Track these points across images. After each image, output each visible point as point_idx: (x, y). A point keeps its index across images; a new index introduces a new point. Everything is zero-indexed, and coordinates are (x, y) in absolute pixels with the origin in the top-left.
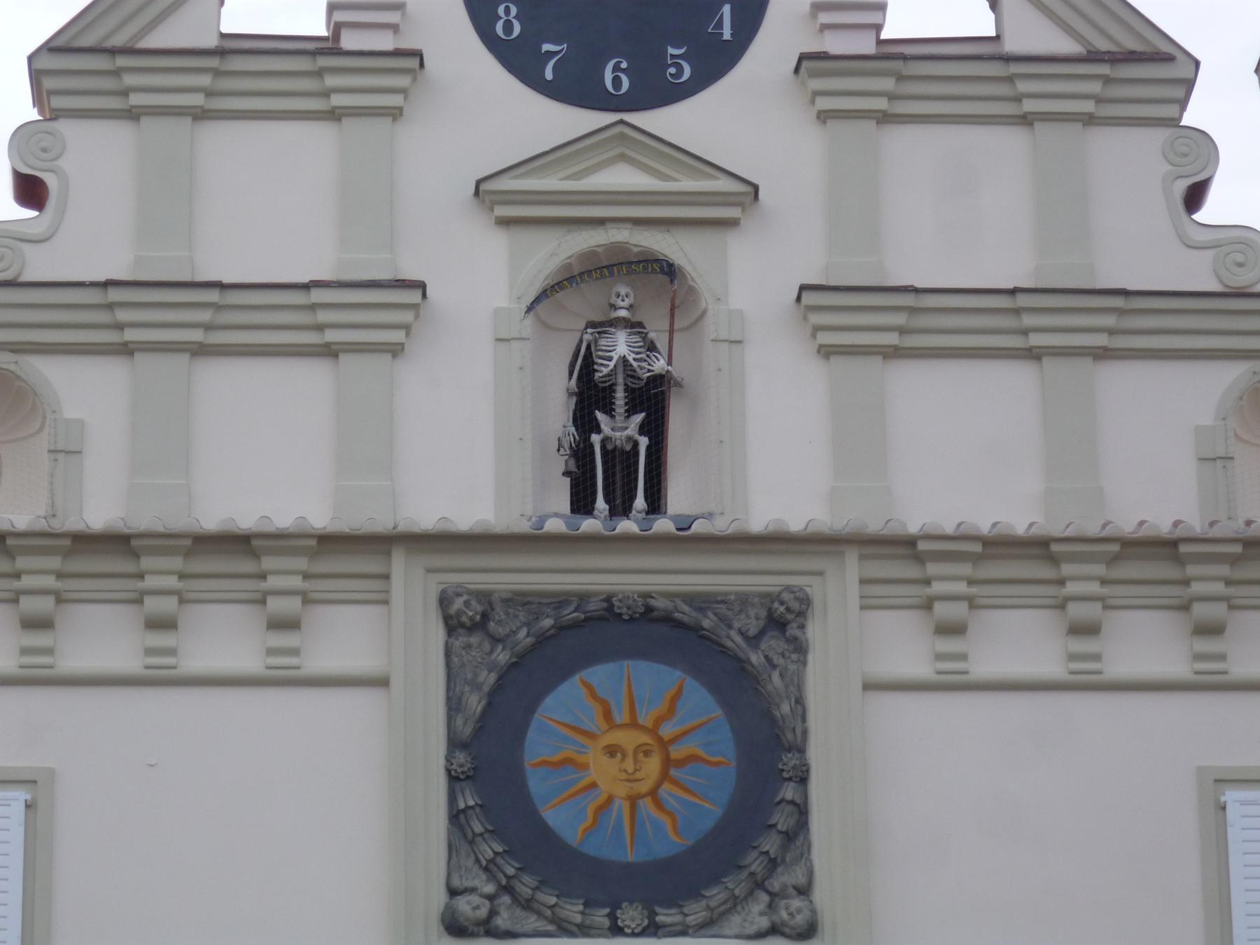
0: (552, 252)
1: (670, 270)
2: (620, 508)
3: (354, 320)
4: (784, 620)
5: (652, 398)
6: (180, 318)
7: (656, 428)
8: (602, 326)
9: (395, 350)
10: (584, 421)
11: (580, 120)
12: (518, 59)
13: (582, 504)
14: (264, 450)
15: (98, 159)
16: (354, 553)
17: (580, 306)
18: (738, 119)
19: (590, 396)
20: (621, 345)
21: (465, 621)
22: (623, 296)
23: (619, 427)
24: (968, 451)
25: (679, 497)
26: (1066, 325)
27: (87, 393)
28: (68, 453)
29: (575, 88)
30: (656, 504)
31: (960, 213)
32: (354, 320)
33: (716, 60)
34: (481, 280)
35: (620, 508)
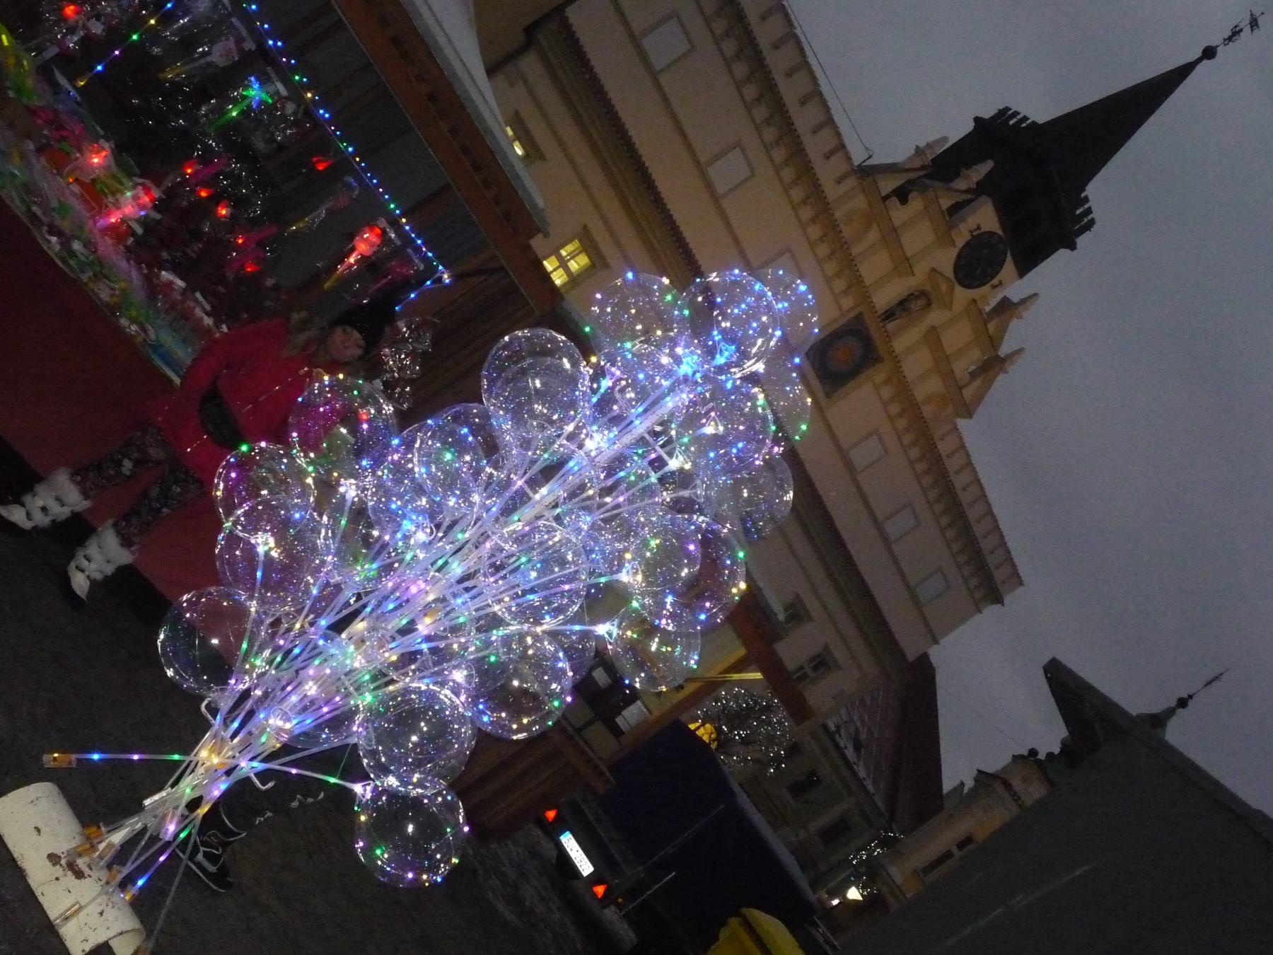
0: (928, 288)
3: (903, 265)
4: (878, 360)
11: (949, 272)
12: (959, 257)
14: (874, 266)
16: (866, 298)
18: (962, 295)
19: (902, 303)
21: (859, 318)
24: (916, 364)
26: (943, 364)
27: (873, 235)
31: (958, 336)
32: (903, 265)
34: (917, 280)
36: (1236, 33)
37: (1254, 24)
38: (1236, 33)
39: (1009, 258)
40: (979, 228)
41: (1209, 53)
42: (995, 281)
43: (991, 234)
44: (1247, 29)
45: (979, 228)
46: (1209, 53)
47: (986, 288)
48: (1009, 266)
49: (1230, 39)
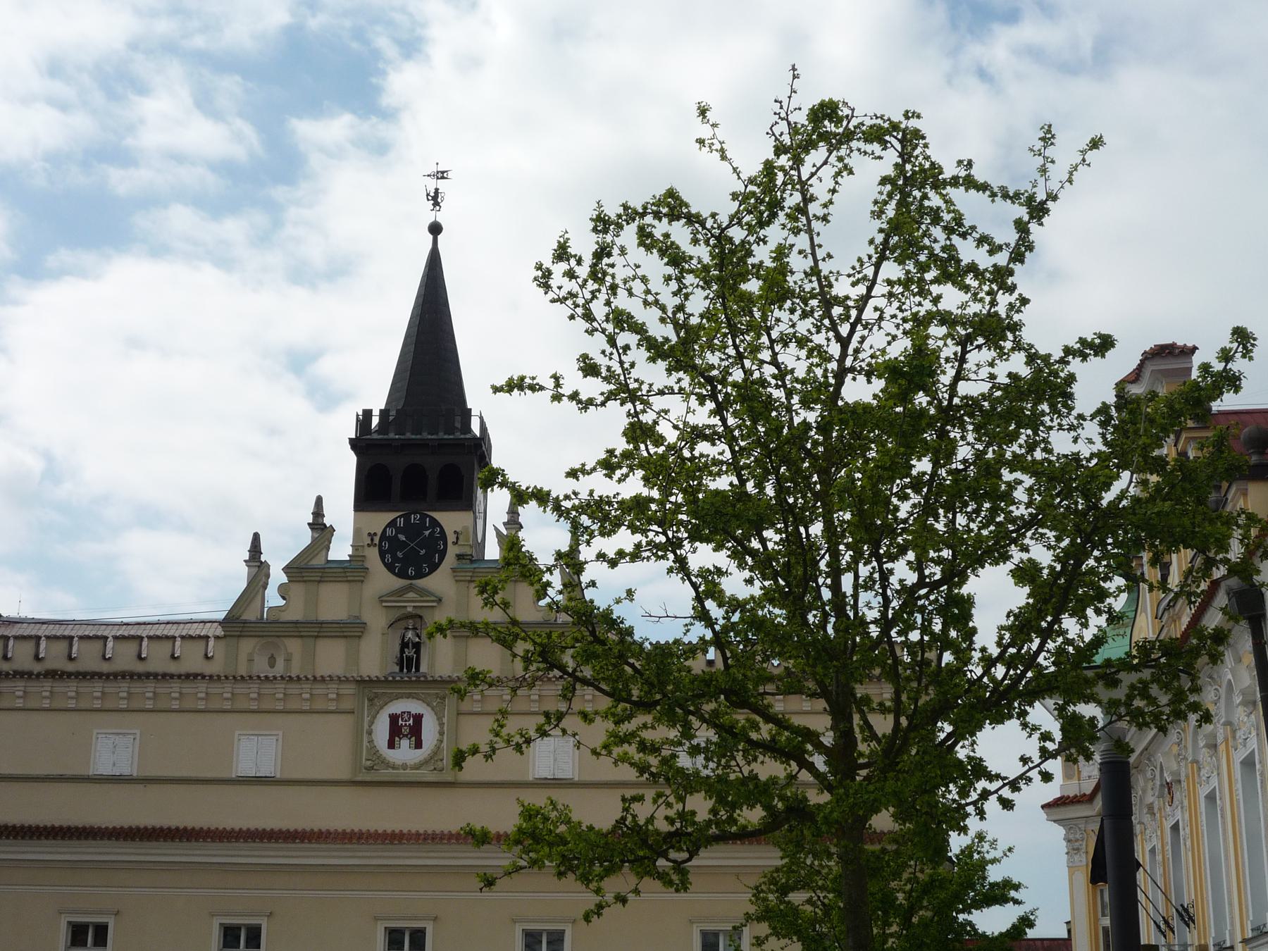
1: (421, 617)
2: (409, 670)
5: (417, 646)
6: (313, 630)
7: (418, 652)
8: (407, 629)
9: (360, 637)
10: (402, 652)
12: (390, 568)
13: (401, 670)
15: (298, 590)
17: (403, 624)
18: (440, 581)
19: (404, 645)
20: (410, 635)
22: (411, 624)
23: (410, 652)
25: (423, 669)
27: (294, 646)
28: (288, 660)
29: (402, 574)
30: (417, 669)
33: (434, 567)
34: (377, 620)
35: (409, 670)
36: (435, 199)
37: (441, 175)
38: (435, 199)
39: (437, 515)
40: (372, 536)
41: (435, 229)
42: (451, 538)
43: (392, 524)
44: (441, 184)
45: (372, 536)
46: (435, 229)
47: (452, 551)
48: (450, 521)
49: (436, 204)
